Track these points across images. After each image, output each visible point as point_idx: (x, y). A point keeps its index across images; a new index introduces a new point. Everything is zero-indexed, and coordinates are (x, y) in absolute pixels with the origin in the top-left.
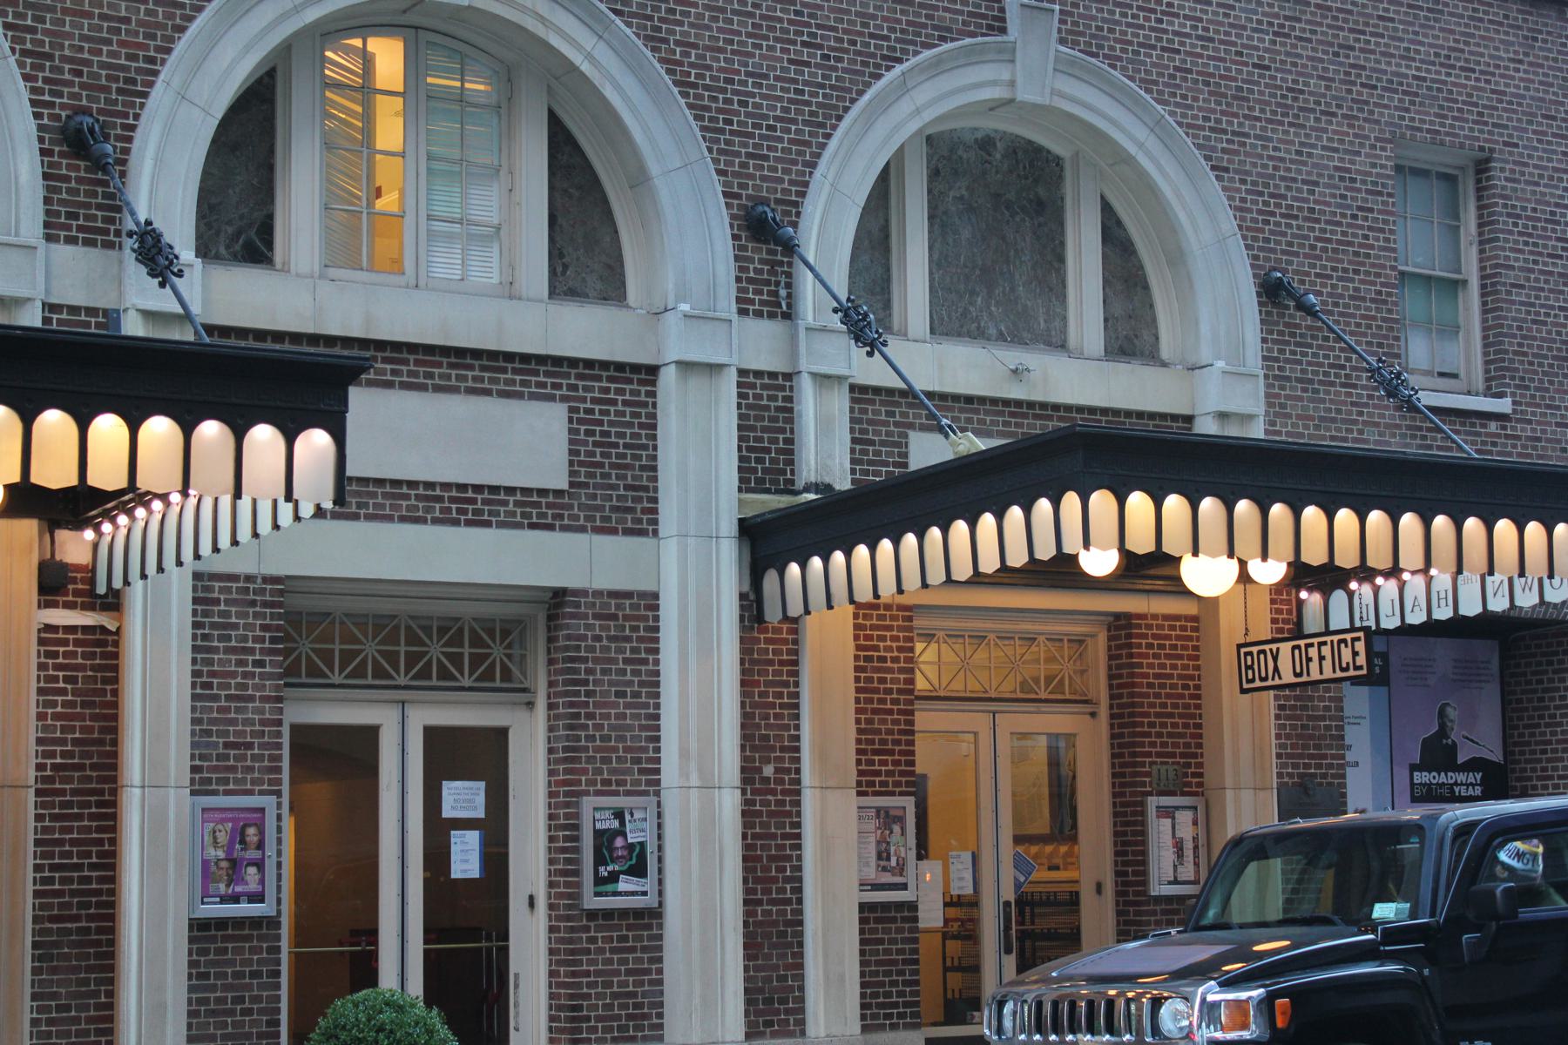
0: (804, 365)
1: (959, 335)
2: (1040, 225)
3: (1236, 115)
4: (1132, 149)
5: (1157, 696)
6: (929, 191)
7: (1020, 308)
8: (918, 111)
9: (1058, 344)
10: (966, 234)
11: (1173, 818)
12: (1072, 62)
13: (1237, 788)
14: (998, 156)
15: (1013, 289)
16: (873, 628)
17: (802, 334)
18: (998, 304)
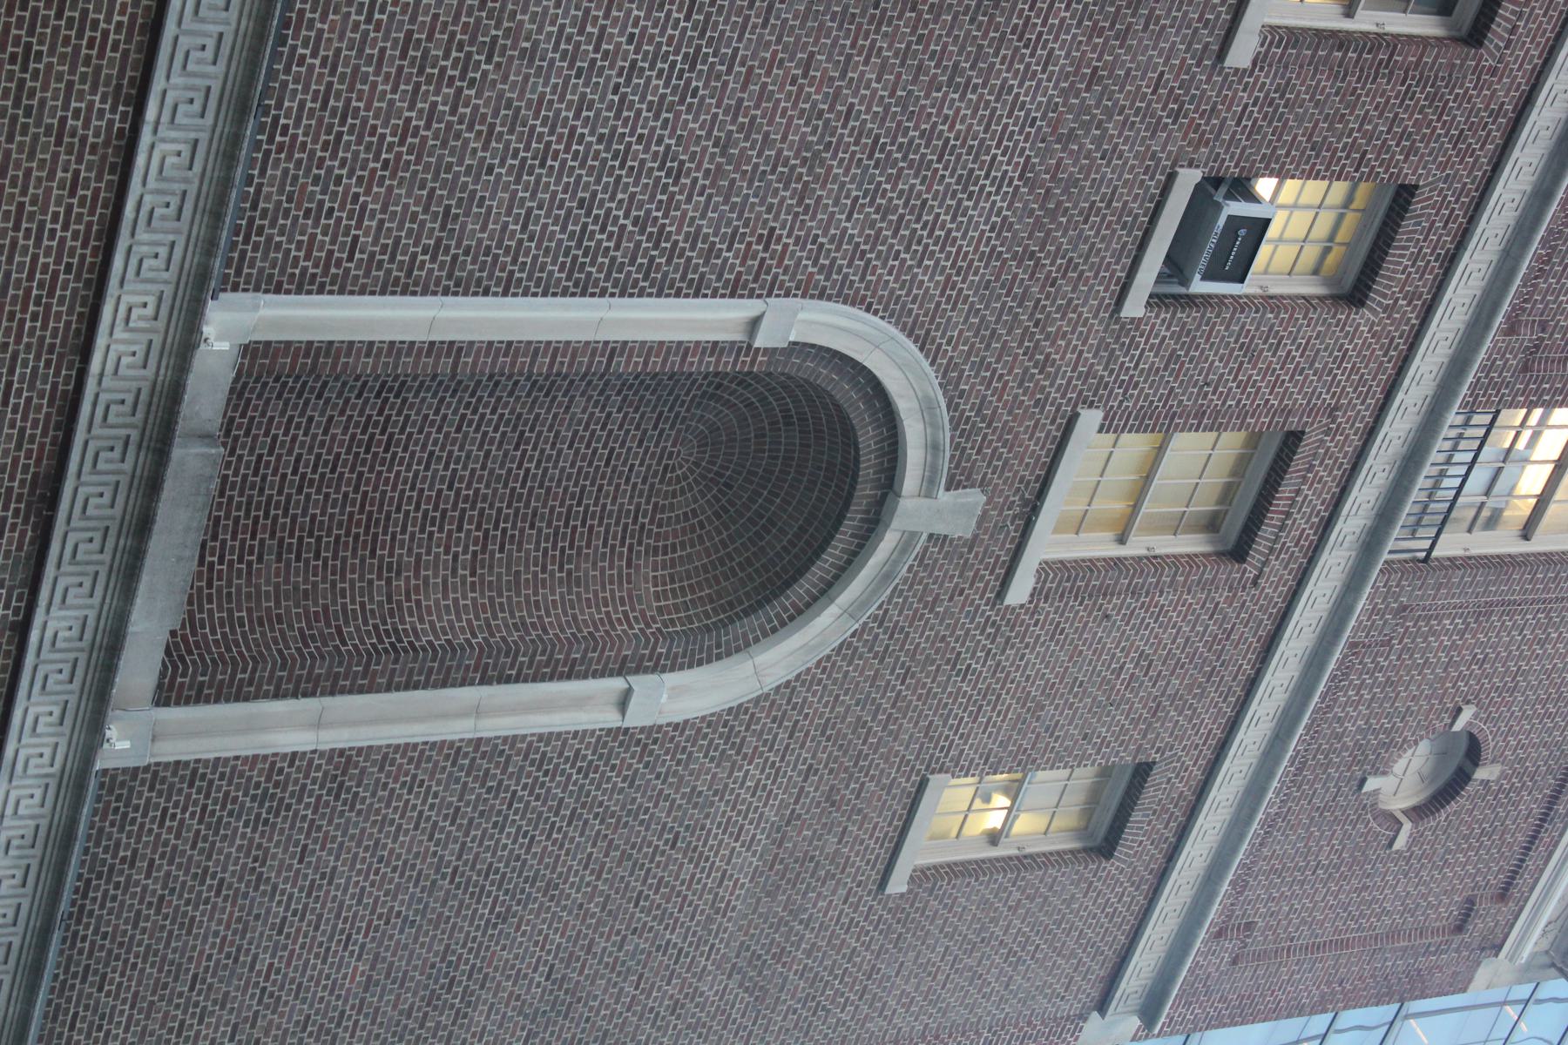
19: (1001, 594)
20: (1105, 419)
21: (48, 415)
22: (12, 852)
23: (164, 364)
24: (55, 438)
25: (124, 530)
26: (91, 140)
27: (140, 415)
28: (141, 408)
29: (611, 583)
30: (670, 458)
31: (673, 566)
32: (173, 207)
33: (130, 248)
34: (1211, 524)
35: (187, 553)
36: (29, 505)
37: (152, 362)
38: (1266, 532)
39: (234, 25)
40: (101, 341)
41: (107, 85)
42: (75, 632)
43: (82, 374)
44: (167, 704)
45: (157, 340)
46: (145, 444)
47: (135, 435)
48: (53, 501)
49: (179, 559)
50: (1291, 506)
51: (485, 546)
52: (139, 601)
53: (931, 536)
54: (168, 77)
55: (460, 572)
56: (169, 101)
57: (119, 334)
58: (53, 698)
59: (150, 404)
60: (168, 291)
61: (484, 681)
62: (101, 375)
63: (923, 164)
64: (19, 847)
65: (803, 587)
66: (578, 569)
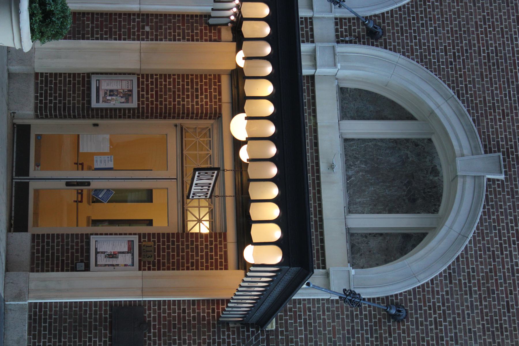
0: (318, 45)
1: (346, 155)
2: (404, 200)
3: (479, 289)
4: (448, 223)
5: (187, 247)
6: (407, 140)
7: (364, 188)
8: (439, 107)
9: (351, 208)
10: (392, 160)
11: (128, 253)
12: (480, 186)
13: (142, 277)
14: (431, 178)
15: (371, 184)
16: (211, 92)
17: (331, 44)
18: (363, 175)
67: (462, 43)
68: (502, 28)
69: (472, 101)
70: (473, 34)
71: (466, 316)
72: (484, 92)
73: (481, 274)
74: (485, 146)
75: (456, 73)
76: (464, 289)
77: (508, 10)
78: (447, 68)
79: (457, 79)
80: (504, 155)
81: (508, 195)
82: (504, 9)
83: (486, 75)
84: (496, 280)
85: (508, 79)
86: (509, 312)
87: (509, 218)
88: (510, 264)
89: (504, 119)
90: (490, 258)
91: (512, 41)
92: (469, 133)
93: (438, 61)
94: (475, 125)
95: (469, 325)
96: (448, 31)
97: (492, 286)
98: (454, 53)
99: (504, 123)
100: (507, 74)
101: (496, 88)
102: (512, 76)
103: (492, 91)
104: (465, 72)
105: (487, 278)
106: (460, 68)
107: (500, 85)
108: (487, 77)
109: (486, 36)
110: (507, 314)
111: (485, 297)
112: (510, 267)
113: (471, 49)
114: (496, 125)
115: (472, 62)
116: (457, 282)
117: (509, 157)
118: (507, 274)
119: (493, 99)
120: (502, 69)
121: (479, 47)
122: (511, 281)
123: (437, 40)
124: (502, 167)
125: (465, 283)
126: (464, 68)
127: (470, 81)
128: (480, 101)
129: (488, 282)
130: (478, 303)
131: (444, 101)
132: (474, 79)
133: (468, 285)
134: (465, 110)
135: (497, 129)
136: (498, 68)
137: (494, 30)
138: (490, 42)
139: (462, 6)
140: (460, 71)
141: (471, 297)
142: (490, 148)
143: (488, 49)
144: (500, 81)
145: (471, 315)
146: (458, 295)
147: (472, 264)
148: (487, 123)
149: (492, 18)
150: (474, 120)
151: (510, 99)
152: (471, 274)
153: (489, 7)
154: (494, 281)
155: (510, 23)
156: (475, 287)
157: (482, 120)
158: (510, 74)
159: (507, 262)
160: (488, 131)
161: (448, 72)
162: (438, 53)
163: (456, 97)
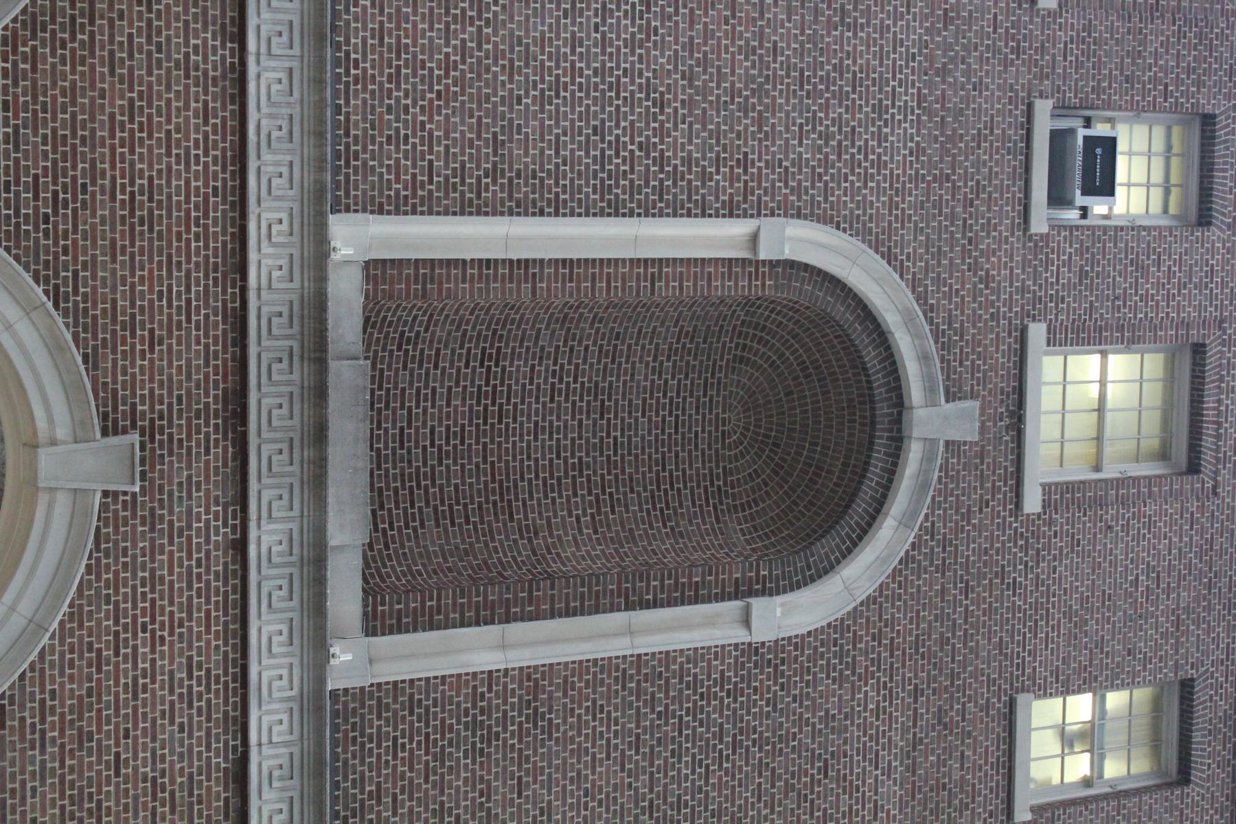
19: (1018, 505)
20: (1049, 333)
21: (224, 331)
22: (276, 784)
23: (306, 276)
24: (234, 353)
25: (306, 442)
26: (211, 73)
27: (296, 328)
28: (296, 319)
29: (708, 534)
30: (724, 425)
31: (753, 519)
32: (285, 130)
33: (259, 168)
34: (1163, 455)
35: (360, 464)
36: (225, 420)
37: (297, 275)
38: (1208, 442)
39: (299, 152)
40: (253, 256)
41: (214, 24)
42: (284, 547)
43: (244, 289)
44: (374, 634)
45: (296, 253)
46: (306, 355)
47: (296, 345)
48: (241, 416)
49: (356, 470)
50: (1218, 416)
51: (599, 508)
52: (331, 514)
53: (947, 443)
54: (259, 14)
55: (585, 531)
56: (263, 34)
57: (266, 249)
58: (279, 616)
59: (302, 316)
60: (296, 207)
61: (629, 607)
62: (259, 289)
63: (841, 96)
64: (281, 778)
65: (860, 507)
66: (678, 525)
67: (74, 168)
68: (168, 132)
69: (86, 310)
70: (103, 145)
71: (29, 794)
72: (114, 290)
73: (69, 702)
74: (105, 417)
75: (56, 244)
76: (28, 737)
77: (187, 86)
78: (37, 230)
79: (56, 258)
80: (142, 434)
81: (143, 524)
82: (178, 83)
83: (123, 247)
84: (99, 710)
85: (170, 256)
86: (117, 774)
87: (140, 574)
88: (131, 674)
89: (152, 351)
90: (90, 665)
91: (187, 164)
92: (71, 390)
93: (17, 214)
94: (87, 369)
95: (33, 811)
96: (45, 136)
97: (89, 725)
98: (55, 193)
99: (152, 361)
100: (170, 245)
101: (142, 278)
102: (179, 249)
103: (133, 286)
104: (75, 242)
105: (80, 710)
106: (66, 232)
107: (151, 271)
108: (123, 253)
109: (132, 152)
110: (114, 780)
111: (71, 750)
112: (130, 681)
113: (94, 183)
114: (133, 365)
115: (94, 215)
116: (16, 723)
117: (152, 440)
118: (122, 696)
119: (133, 305)
120: (160, 233)
121: (113, 178)
122: (130, 711)
123: (17, 160)
124: (137, 460)
125: (33, 725)
126: (75, 232)
127: (85, 263)
128: (104, 310)
129: (80, 719)
130: (57, 764)
131: (22, 313)
132: (94, 257)
133: (38, 727)
134: (69, 337)
135: (133, 375)
136: (151, 230)
137: (150, 137)
138: (139, 166)
139: (83, 74)
140: (66, 238)
141: (43, 752)
142: (115, 421)
143: (132, 184)
144: (151, 261)
145: (39, 790)
146: (15, 750)
147: (53, 682)
148: (115, 361)
149: (150, 106)
150: (85, 358)
151: (170, 305)
152: (49, 703)
153: (146, 78)
154: (94, 714)
155: (187, 118)
156: (53, 730)
157: (105, 355)
158: (175, 244)
159: (126, 671)
160: (115, 382)
161: (37, 240)
162: (17, 194)
163: (50, 305)
